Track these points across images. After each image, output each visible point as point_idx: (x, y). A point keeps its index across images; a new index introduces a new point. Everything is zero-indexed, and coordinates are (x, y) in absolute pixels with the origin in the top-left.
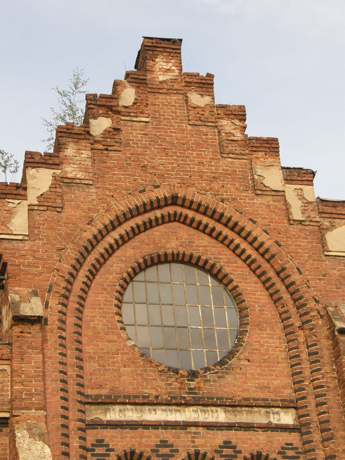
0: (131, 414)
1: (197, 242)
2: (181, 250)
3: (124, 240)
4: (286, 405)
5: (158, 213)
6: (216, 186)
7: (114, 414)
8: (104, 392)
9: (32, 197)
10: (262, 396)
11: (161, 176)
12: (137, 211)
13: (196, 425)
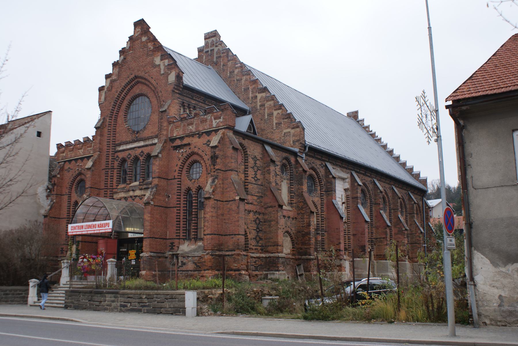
3: (126, 94)
4: (156, 137)
5: (133, 83)
7: (122, 148)
8: (119, 142)
12: (128, 84)
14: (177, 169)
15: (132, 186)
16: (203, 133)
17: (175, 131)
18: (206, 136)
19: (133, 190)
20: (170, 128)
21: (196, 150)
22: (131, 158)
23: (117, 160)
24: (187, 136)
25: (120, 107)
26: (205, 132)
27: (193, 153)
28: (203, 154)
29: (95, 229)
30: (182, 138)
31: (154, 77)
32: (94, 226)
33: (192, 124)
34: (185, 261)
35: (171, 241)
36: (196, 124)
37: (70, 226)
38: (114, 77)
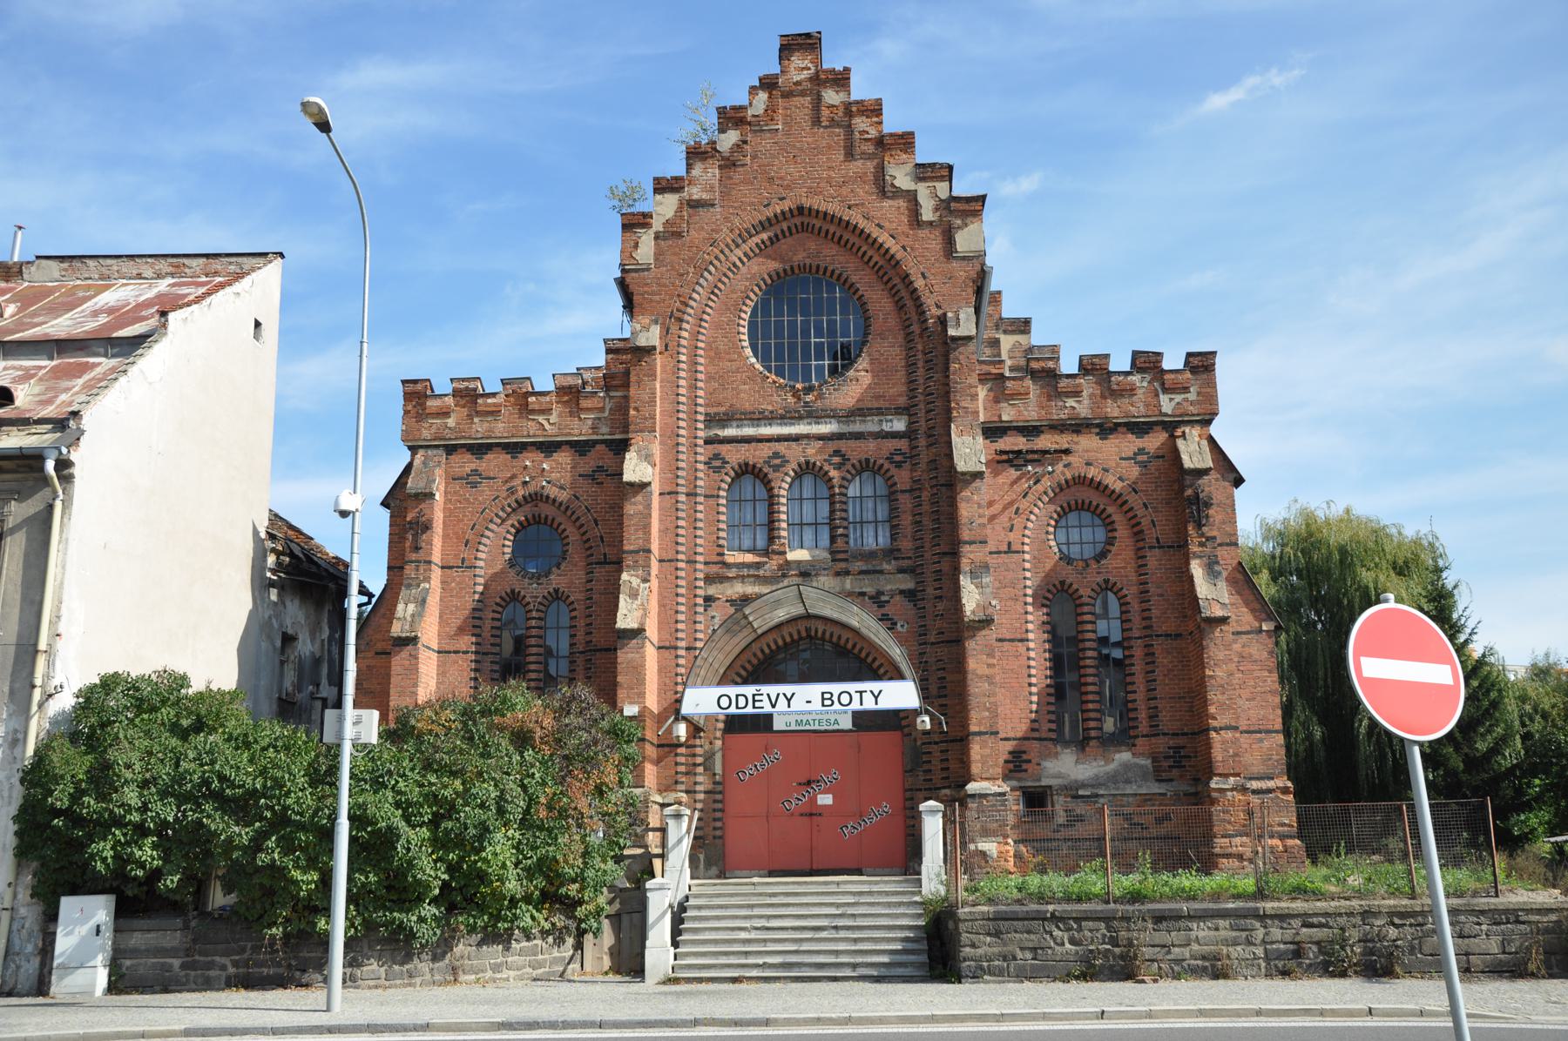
0: (749, 431)
1: (825, 252)
2: (808, 261)
4: (898, 411)
6: (845, 190)
9: (657, 225)
11: (788, 187)
13: (808, 437)
21: (1092, 472)
30: (1030, 431)
31: (886, 224)
33: (1076, 394)
36: (1091, 396)
38: (696, 193)
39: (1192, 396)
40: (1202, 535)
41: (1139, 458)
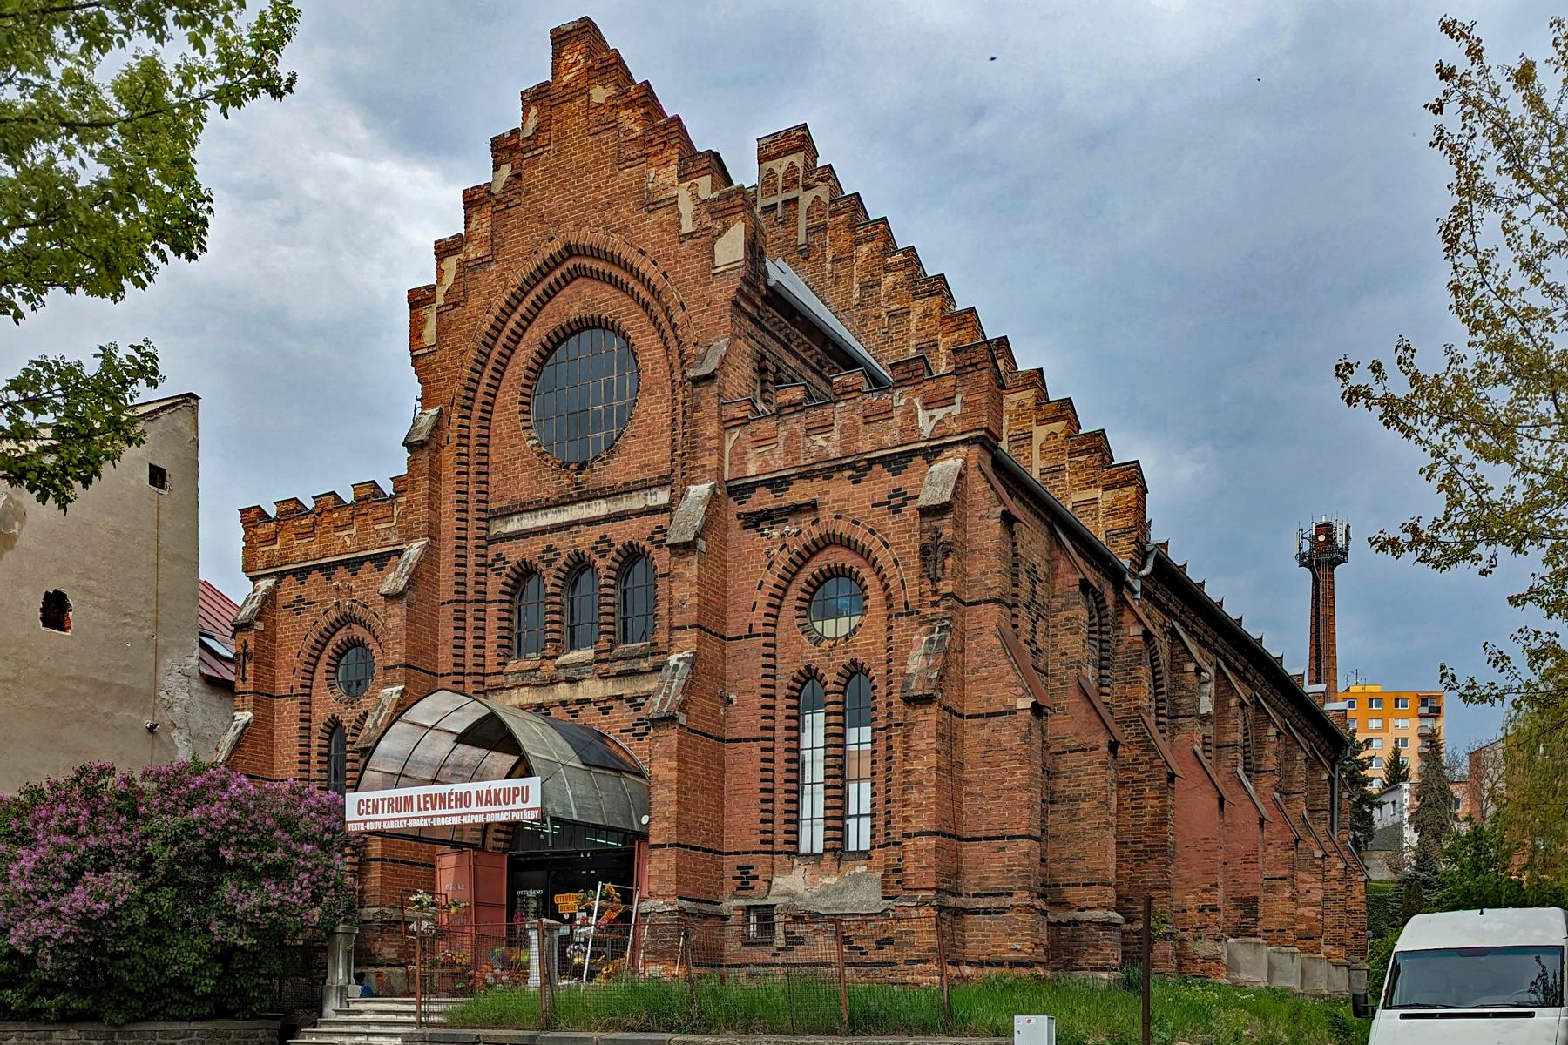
7: (514, 525)
8: (505, 503)
10: (641, 477)
13: (576, 523)
14: (762, 598)
15: (565, 666)
16: (872, 462)
17: (751, 454)
18: (886, 476)
19: (571, 681)
20: (728, 446)
21: (842, 527)
22: (560, 563)
23: (498, 571)
24: (802, 476)
25: (500, 370)
26: (882, 460)
27: (829, 541)
28: (873, 544)
29: (464, 810)
30: (779, 484)
32: (462, 800)
33: (826, 427)
34: (800, 930)
35: (740, 860)
36: (843, 428)
37: (352, 799)
39: (956, 410)
40: (936, 593)
41: (894, 502)
